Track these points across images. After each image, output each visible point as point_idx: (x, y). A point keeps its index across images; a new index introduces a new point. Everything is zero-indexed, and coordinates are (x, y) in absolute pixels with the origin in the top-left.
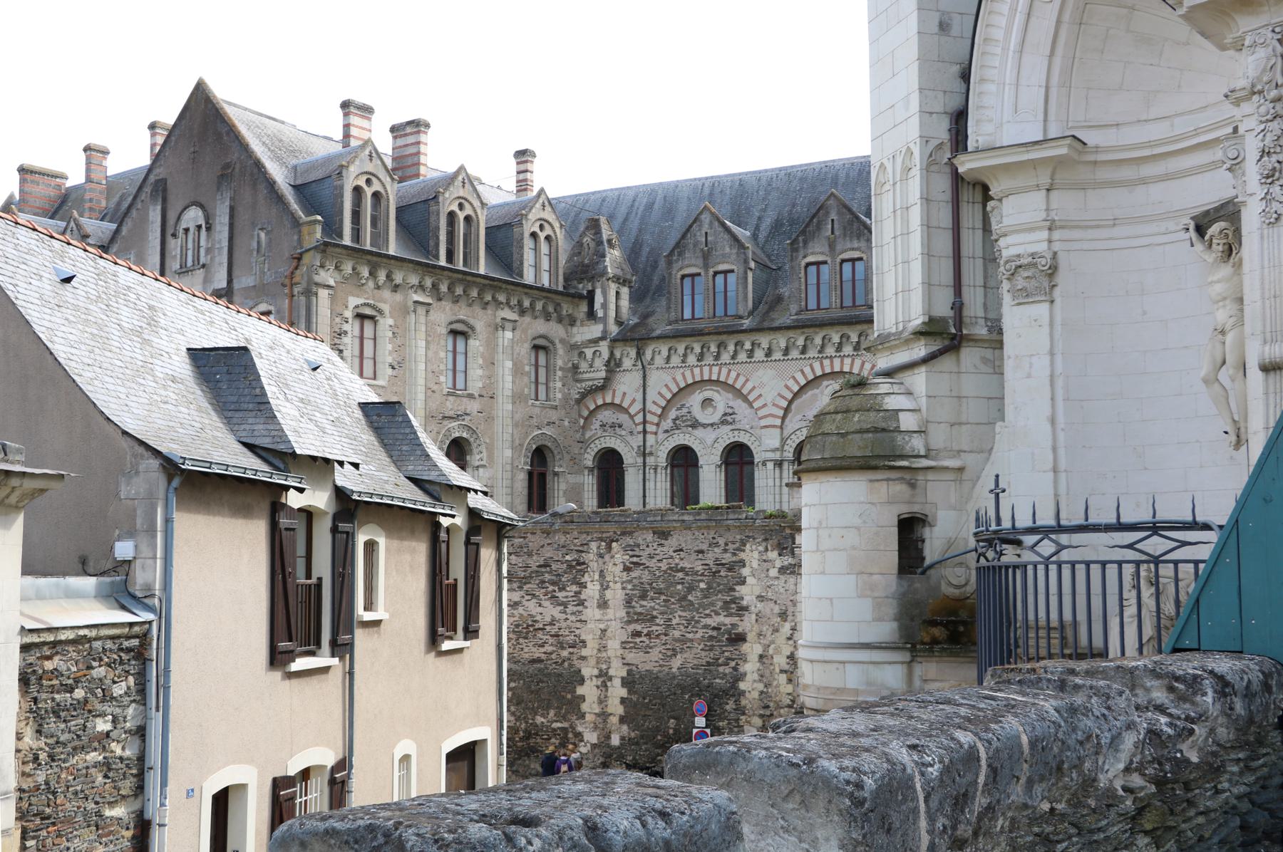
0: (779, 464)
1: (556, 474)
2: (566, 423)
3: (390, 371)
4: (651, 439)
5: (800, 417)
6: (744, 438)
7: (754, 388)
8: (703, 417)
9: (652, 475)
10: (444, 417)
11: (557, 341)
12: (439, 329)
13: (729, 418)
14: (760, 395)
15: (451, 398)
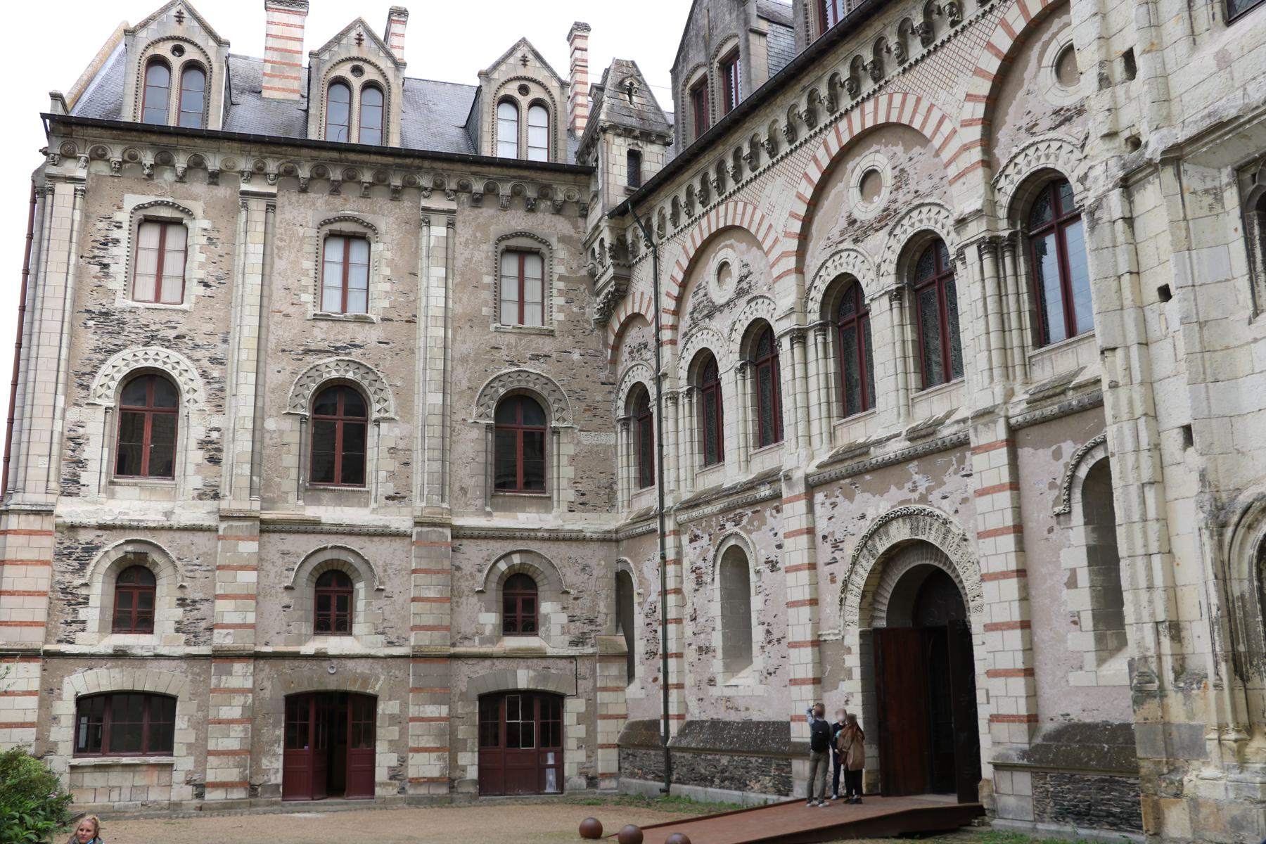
0: (799, 336)
1: (556, 432)
2: (576, 356)
3: (201, 290)
4: (666, 351)
5: (823, 243)
6: (761, 311)
7: (763, 216)
8: (720, 295)
9: (671, 409)
10: (307, 352)
11: (554, 241)
12: (301, 231)
13: (744, 285)
14: (771, 226)
15: (322, 324)
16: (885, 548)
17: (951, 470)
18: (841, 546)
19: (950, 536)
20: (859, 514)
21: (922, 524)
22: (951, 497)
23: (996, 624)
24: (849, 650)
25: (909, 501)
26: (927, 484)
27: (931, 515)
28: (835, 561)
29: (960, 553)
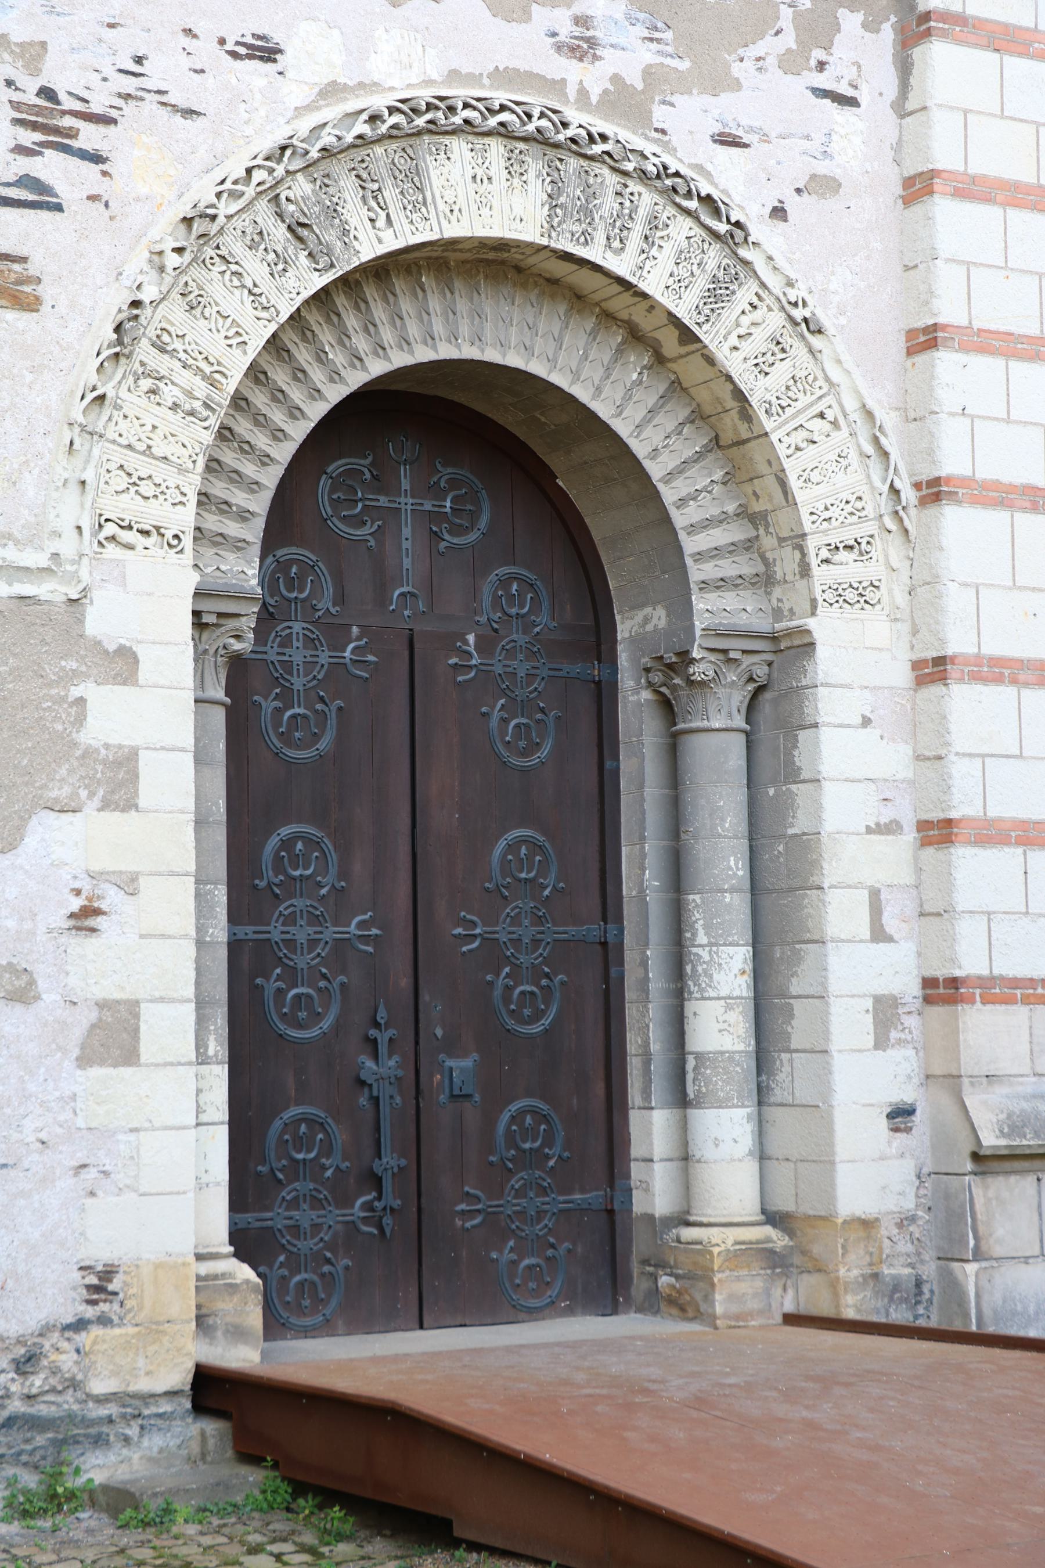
16: (392, 243)
17: (769, 46)
18: (89, 136)
19: (745, 294)
20: (241, 28)
21: (608, 204)
22: (758, 148)
23: (995, 662)
24: (122, 664)
25: (558, 86)
26: (648, 55)
27: (670, 184)
28: (41, 198)
29: (781, 373)
